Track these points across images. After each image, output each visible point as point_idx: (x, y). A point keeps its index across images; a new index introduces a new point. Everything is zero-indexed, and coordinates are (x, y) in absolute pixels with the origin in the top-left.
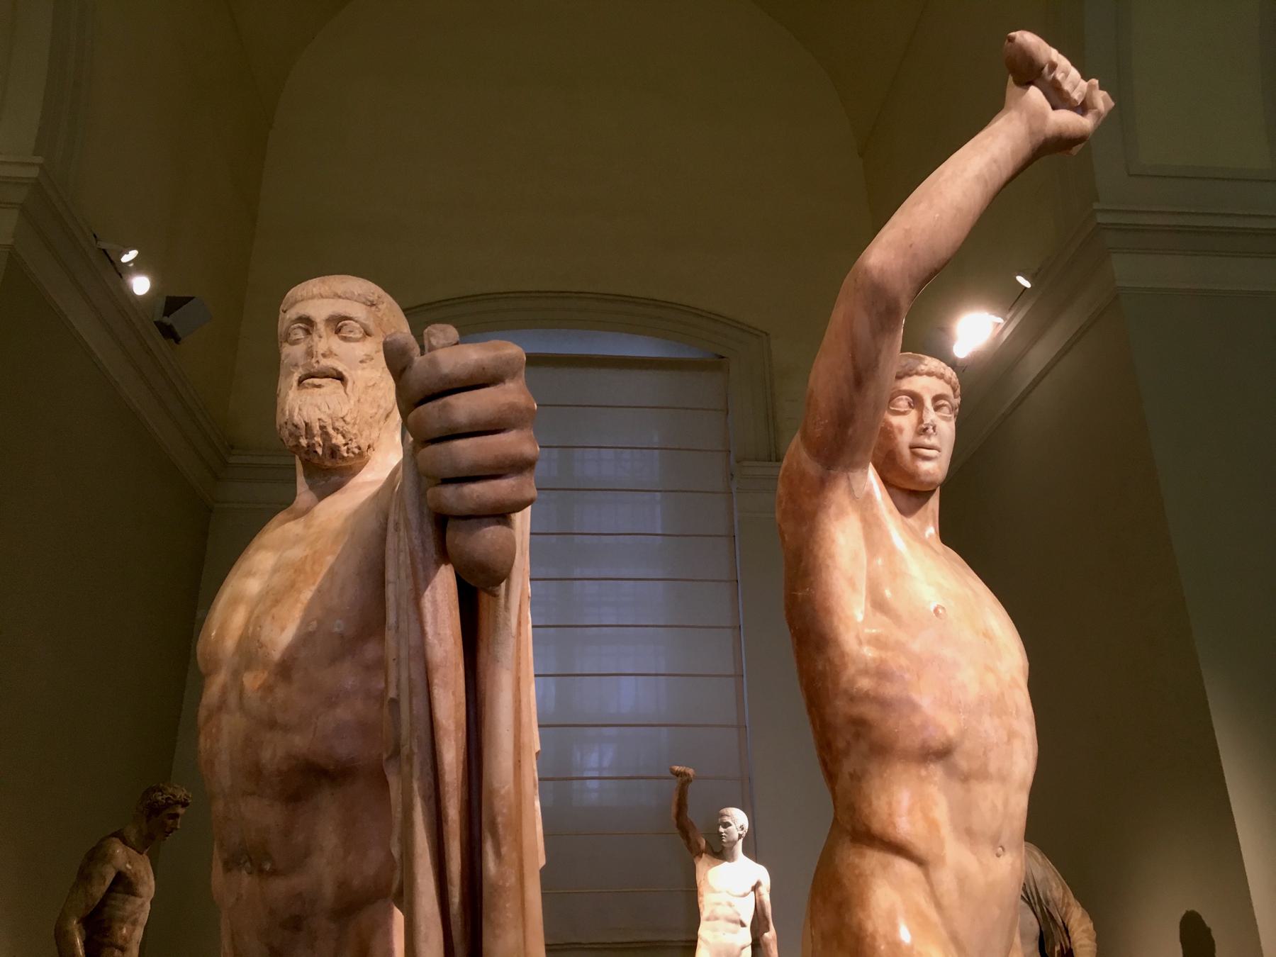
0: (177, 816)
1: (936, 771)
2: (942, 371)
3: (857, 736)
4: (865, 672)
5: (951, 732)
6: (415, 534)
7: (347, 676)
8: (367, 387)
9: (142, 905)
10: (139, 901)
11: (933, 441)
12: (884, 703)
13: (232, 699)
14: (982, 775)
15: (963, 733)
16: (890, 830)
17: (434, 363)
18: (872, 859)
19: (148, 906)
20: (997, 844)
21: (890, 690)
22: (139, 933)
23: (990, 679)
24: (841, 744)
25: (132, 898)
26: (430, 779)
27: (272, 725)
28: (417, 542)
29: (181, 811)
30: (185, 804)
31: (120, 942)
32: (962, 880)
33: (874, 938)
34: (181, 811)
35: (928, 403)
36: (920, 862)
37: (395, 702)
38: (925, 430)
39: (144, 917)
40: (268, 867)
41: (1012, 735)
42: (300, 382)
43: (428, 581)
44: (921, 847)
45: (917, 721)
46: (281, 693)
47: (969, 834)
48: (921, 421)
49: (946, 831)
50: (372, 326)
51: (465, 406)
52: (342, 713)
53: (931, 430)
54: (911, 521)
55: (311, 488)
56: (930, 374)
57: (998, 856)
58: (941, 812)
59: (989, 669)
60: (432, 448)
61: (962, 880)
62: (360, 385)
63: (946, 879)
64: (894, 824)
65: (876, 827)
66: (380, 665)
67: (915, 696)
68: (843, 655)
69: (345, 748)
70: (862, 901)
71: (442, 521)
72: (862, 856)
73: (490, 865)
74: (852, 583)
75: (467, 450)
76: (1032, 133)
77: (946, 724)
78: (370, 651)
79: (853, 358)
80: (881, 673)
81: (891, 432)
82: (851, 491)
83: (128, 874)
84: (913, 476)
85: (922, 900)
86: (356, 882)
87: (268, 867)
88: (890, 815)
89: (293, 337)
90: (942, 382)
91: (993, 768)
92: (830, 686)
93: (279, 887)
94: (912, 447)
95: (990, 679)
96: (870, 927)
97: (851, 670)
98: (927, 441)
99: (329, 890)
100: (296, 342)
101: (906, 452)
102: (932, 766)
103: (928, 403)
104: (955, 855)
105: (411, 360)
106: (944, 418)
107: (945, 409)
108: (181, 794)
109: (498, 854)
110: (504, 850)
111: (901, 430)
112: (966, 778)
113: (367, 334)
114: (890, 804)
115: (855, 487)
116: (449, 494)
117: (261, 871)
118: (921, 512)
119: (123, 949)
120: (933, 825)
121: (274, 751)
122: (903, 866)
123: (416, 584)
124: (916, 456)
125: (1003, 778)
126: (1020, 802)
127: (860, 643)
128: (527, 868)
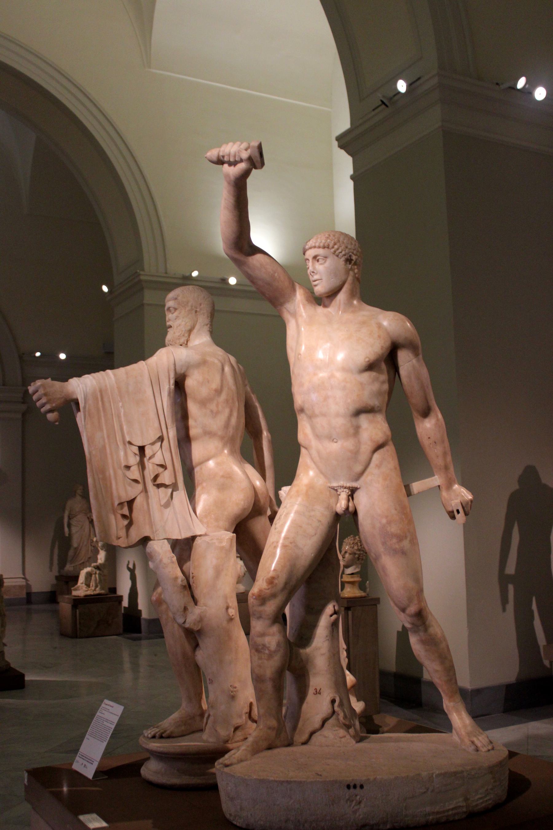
2: (313, 245)
8: (177, 327)
11: (316, 277)
20: (331, 438)
32: (319, 452)
41: (326, 398)
47: (318, 437)
50: (176, 306)
54: (329, 309)
56: (310, 248)
61: (319, 452)
62: (175, 327)
63: (314, 453)
76: (229, 183)
90: (316, 249)
91: (317, 411)
106: (321, 264)
113: (176, 309)
118: (333, 302)
125: (324, 415)
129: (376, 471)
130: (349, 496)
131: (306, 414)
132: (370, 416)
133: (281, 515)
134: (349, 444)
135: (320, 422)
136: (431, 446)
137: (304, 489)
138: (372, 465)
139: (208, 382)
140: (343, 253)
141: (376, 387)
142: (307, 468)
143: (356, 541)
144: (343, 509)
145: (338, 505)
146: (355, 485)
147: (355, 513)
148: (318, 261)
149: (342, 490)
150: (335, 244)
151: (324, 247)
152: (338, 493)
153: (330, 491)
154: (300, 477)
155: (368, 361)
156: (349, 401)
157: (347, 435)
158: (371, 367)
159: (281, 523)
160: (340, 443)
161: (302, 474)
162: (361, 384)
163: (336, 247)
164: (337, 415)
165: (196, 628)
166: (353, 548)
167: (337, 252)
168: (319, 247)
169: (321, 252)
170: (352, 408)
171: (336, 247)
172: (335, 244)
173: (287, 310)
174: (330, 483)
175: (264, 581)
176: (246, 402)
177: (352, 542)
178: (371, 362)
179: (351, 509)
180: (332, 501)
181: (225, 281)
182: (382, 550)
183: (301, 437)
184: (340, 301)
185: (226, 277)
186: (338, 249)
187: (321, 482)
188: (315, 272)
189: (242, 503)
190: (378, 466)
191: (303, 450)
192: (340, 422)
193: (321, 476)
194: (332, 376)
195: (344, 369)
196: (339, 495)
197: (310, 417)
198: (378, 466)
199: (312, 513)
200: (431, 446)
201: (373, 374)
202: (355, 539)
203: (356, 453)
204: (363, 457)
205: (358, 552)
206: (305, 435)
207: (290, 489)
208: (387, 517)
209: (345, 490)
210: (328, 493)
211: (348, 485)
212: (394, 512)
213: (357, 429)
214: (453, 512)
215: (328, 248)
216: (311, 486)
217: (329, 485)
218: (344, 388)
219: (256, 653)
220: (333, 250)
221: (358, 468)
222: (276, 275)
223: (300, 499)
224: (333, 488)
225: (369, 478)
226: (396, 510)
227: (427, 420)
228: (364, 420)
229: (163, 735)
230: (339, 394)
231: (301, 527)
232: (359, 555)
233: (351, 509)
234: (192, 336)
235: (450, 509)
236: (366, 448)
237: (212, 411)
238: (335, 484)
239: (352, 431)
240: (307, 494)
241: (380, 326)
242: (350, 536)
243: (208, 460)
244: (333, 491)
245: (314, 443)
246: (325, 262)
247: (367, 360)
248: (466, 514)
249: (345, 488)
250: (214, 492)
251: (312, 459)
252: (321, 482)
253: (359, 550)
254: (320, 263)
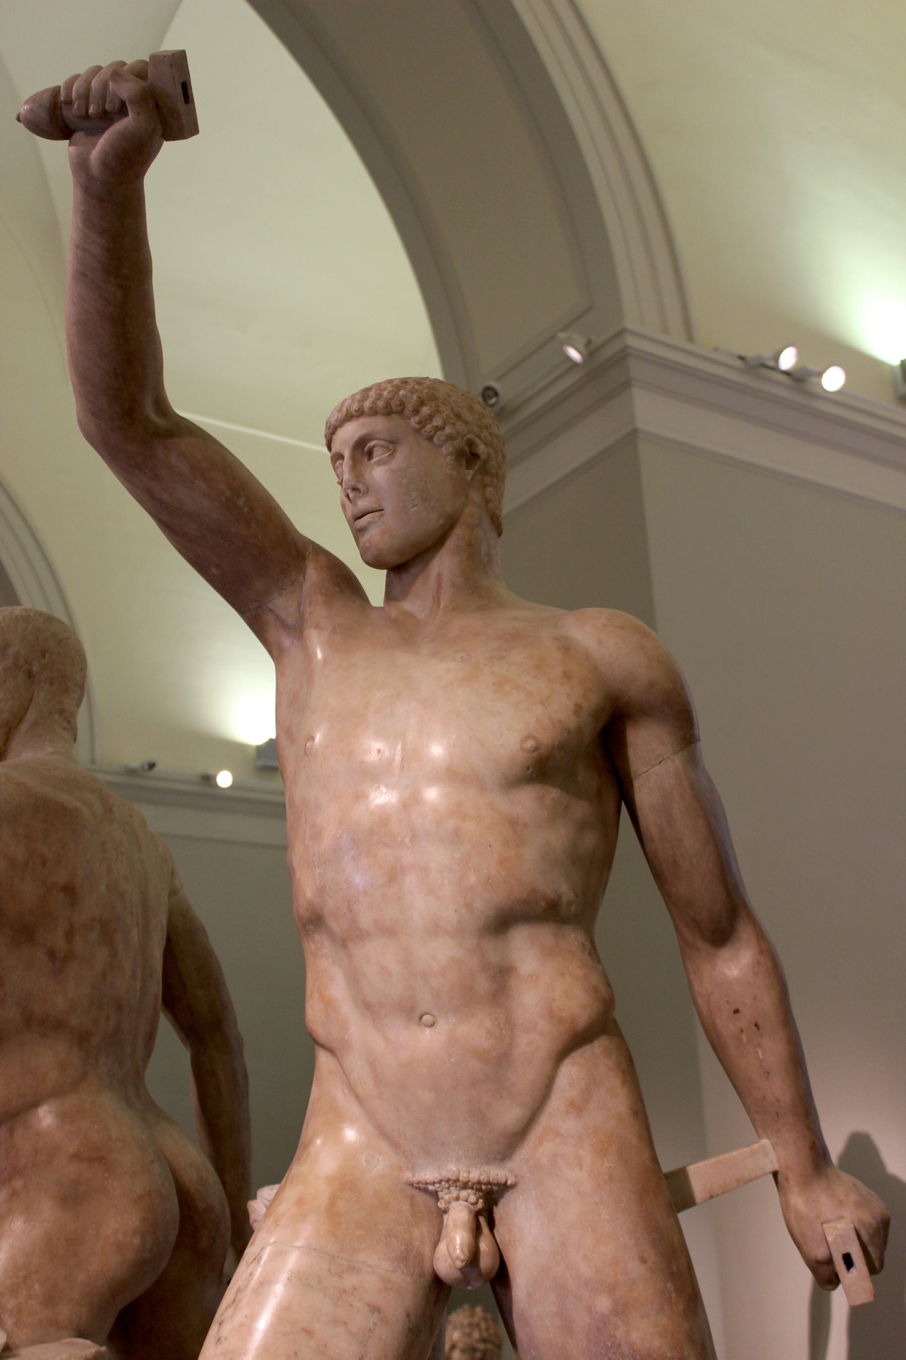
20: (413, 1013)
32: (373, 1064)
36: (331, 1051)
41: (394, 875)
47: (369, 1008)
49: (347, 1009)
61: (373, 1064)
63: (356, 1064)
90: (362, 420)
91: (365, 920)
106: (379, 463)
115: (283, 615)
129: (570, 1125)
130: (477, 1214)
131: (330, 933)
132: (544, 933)
133: (239, 1290)
134: (475, 1030)
135: (377, 956)
136: (744, 1036)
137: (322, 1191)
138: (556, 1103)
139: (44, 864)
140: (448, 430)
141: (558, 837)
142: (338, 1118)
143: (476, 1319)
144: (459, 1264)
145: (442, 1247)
146: (497, 1173)
147: (501, 1277)
148: (370, 454)
149: (454, 1192)
150: (422, 403)
151: (388, 412)
152: (441, 1205)
153: (412, 1199)
154: (312, 1149)
155: (536, 749)
156: (472, 879)
157: (465, 999)
158: (541, 769)
159: (239, 1318)
160: (443, 1026)
161: (319, 1142)
162: (513, 823)
163: (425, 410)
164: (434, 929)
166: (469, 1335)
167: (428, 427)
168: (374, 412)
169: (378, 424)
170: (484, 904)
171: (425, 410)
172: (422, 403)
173: (278, 617)
174: (413, 1168)
176: (169, 939)
177: (466, 1321)
178: (543, 751)
179: (486, 1262)
180: (421, 1233)
181: (208, 780)
183: (314, 1014)
184: (439, 576)
185: (211, 772)
186: (431, 417)
187: (380, 1165)
188: (360, 486)
189: (137, 1241)
190: (577, 1108)
191: (323, 1059)
192: (441, 954)
193: (384, 1146)
194: (412, 801)
195: (452, 775)
196: (445, 1211)
197: (343, 943)
198: (577, 1108)
199: (350, 1281)
200: (744, 1036)
201: (553, 793)
202: (473, 1315)
203: (498, 1060)
204: (525, 1075)
205: (481, 1346)
206: (329, 1004)
207: (277, 1195)
208: (612, 1289)
209: (464, 1193)
210: (406, 1207)
211: (475, 1175)
212: (636, 1269)
213: (502, 976)
214: (830, 1261)
215: (401, 413)
216: (346, 1184)
217: (408, 1176)
218: (456, 837)
220: (414, 421)
221: (509, 1115)
222: (241, 502)
223: (307, 1232)
224: (422, 1188)
225: (548, 1147)
226: (643, 1261)
227: (725, 953)
228: (527, 951)
230: (438, 857)
231: (308, 1332)
232: (485, 1352)
233: (486, 1262)
234: (15, 745)
235: (820, 1253)
236: (534, 1041)
237: (51, 954)
238: (428, 1174)
239: (483, 985)
240: (332, 1212)
241: (566, 647)
242: (461, 1305)
243: (36, 1104)
244: (421, 1198)
245: (358, 1031)
246: (393, 454)
247: (530, 744)
248: (873, 1270)
249: (465, 1186)
250: (48, 1211)
251: (351, 1088)
252: (380, 1165)
253: (484, 1340)
254: (375, 459)
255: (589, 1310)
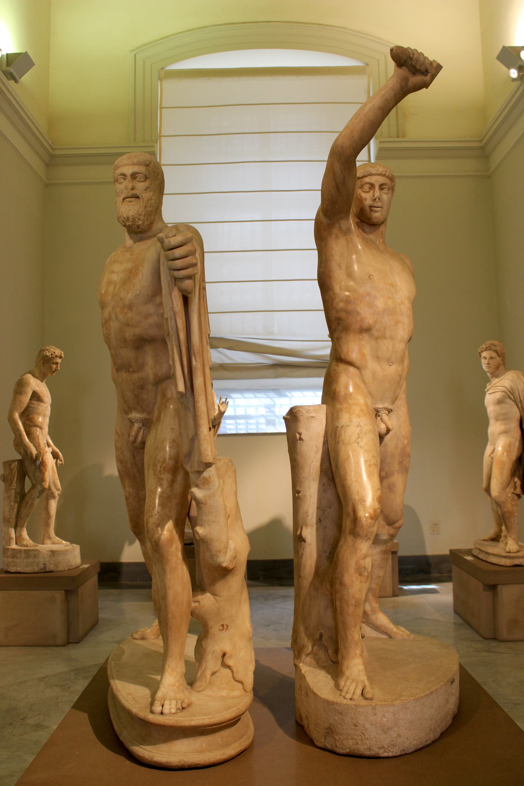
0: (57, 363)
1: (366, 336)
3: (339, 324)
4: (341, 301)
5: (371, 322)
6: (169, 277)
7: (151, 308)
8: (148, 200)
9: (47, 407)
10: (45, 405)
11: (379, 204)
12: (348, 312)
13: (113, 316)
14: (384, 337)
15: (376, 322)
16: (347, 357)
17: (170, 242)
18: (342, 367)
19: (49, 408)
20: (389, 362)
21: (350, 307)
22: (47, 420)
23: (390, 302)
24: (333, 327)
25: (41, 404)
26: (177, 342)
27: (128, 325)
28: (169, 279)
29: (59, 361)
30: (61, 357)
31: (39, 424)
33: (339, 393)
34: (59, 361)
35: (377, 188)
36: (358, 368)
37: (167, 319)
38: (375, 199)
39: (48, 412)
40: (131, 370)
41: (397, 322)
42: (124, 199)
43: (173, 290)
44: (358, 363)
45: (359, 318)
46: (130, 314)
47: (378, 358)
48: (374, 196)
51: (178, 252)
52: (151, 321)
53: (377, 200)
54: (371, 236)
55: (131, 238)
57: (390, 366)
58: (367, 350)
59: (389, 298)
60: (171, 262)
63: (367, 374)
64: (349, 355)
65: (343, 356)
66: (161, 304)
67: (359, 309)
68: (334, 294)
69: (153, 332)
70: (337, 382)
71: (176, 280)
72: (338, 366)
73: (194, 363)
74: (340, 266)
75: (179, 263)
77: (369, 320)
78: (158, 300)
79: (335, 179)
80: (347, 301)
81: (362, 200)
82: (340, 228)
83: (38, 392)
84: (369, 219)
85: (358, 381)
86: (160, 374)
87: (131, 370)
88: (348, 352)
89: (119, 181)
90: (384, 178)
91: (388, 334)
92: (330, 305)
93: (136, 376)
94: (371, 207)
95: (390, 302)
96: (338, 390)
97: (337, 300)
98: (376, 205)
99: (151, 377)
100: (120, 183)
101: (368, 209)
102: (364, 334)
103: (377, 188)
104: (372, 365)
105: (164, 240)
106: (385, 193)
107: (386, 189)
108: (58, 352)
109: (196, 360)
110: (197, 359)
111: (366, 200)
112: (377, 339)
114: (348, 348)
116: (176, 273)
117: (129, 371)
119: (41, 428)
120: (363, 355)
121: (129, 333)
122: (352, 369)
123: (170, 291)
124: (371, 210)
125: (392, 338)
126: (401, 346)
127: (341, 289)
128: (206, 365)
165: (231, 567)
175: (375, 501)
182: (397, 468)
217: (374, 406)
219: (359, 577)
229: (184, 706)
238: (380, 406)
255: (403, 443)
